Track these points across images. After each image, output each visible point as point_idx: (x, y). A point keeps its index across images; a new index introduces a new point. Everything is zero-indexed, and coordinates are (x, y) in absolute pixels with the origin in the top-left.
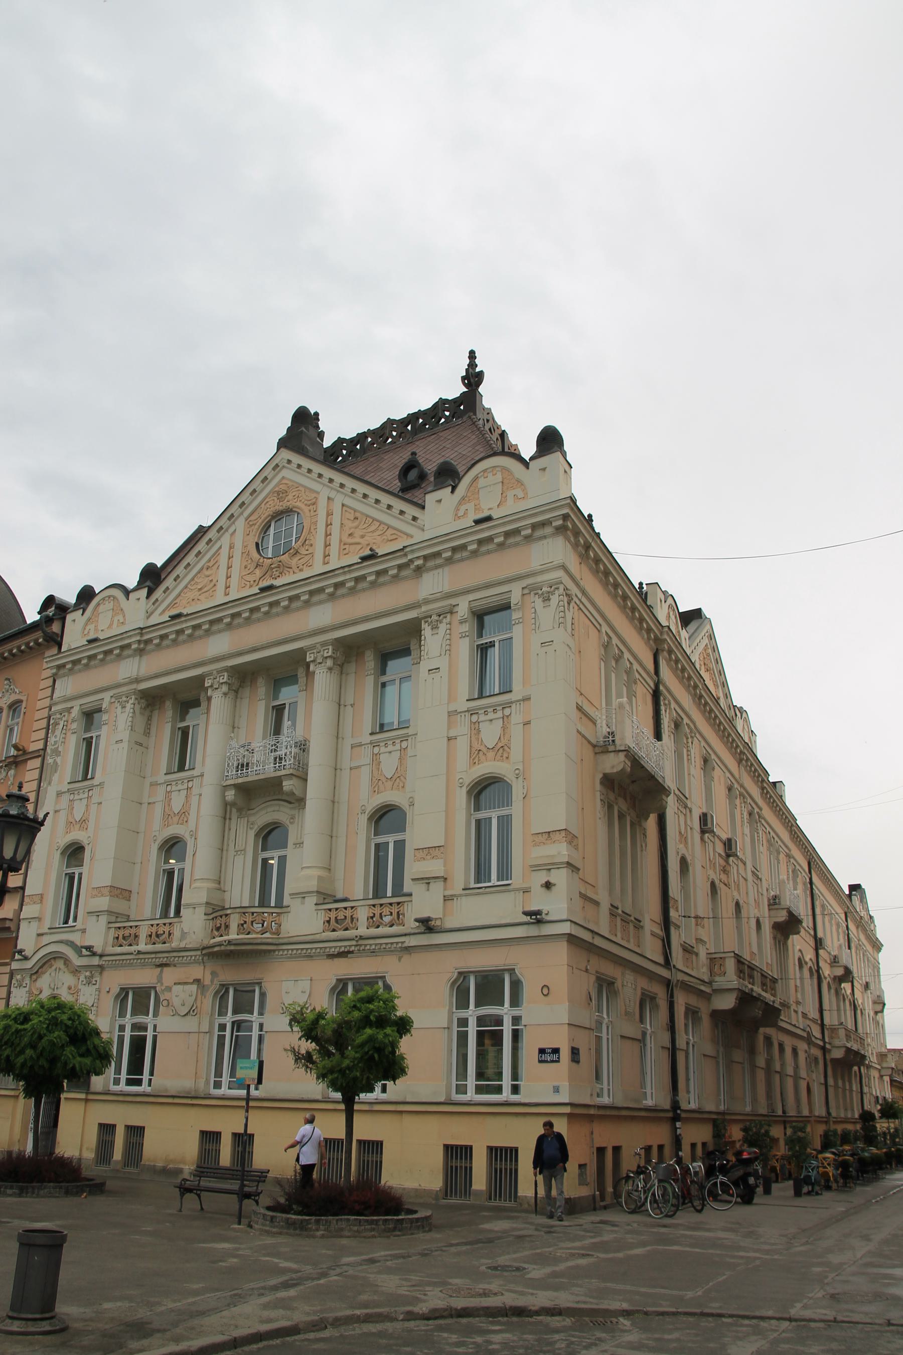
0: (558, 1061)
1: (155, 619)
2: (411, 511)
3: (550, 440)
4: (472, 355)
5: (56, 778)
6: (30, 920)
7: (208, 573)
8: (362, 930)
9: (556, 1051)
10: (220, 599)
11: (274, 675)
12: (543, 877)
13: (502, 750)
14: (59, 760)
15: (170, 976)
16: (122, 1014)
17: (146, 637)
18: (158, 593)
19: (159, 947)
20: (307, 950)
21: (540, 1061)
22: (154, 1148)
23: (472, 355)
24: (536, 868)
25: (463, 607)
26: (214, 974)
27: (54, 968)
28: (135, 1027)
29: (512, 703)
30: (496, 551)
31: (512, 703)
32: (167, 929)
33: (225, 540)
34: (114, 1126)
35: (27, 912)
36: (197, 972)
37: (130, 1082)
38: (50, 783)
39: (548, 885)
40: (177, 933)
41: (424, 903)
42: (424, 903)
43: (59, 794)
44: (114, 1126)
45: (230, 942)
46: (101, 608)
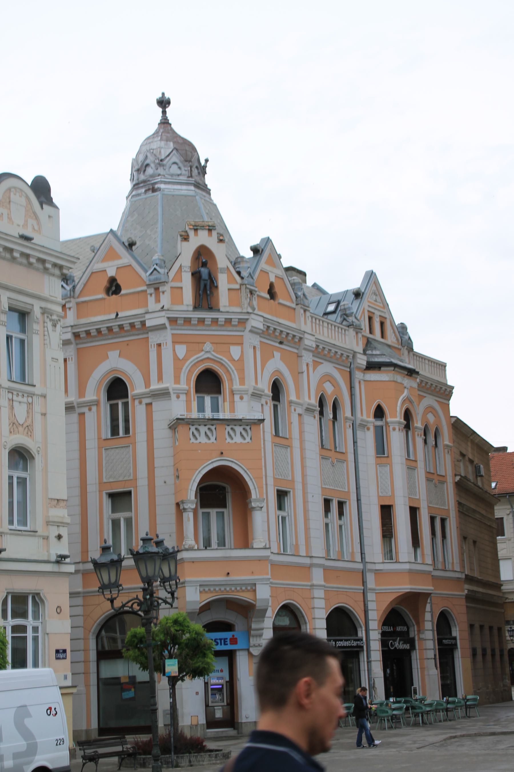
0: (65, 658)
3: (41, 188)
9: (65, 651)
12: (54, 531)
13: (29, 429)
21: (57, 658)
24: (48, 523)
29: (34, 395)
30: (25, 266)
31: (34, 395)
39: (59, 537)
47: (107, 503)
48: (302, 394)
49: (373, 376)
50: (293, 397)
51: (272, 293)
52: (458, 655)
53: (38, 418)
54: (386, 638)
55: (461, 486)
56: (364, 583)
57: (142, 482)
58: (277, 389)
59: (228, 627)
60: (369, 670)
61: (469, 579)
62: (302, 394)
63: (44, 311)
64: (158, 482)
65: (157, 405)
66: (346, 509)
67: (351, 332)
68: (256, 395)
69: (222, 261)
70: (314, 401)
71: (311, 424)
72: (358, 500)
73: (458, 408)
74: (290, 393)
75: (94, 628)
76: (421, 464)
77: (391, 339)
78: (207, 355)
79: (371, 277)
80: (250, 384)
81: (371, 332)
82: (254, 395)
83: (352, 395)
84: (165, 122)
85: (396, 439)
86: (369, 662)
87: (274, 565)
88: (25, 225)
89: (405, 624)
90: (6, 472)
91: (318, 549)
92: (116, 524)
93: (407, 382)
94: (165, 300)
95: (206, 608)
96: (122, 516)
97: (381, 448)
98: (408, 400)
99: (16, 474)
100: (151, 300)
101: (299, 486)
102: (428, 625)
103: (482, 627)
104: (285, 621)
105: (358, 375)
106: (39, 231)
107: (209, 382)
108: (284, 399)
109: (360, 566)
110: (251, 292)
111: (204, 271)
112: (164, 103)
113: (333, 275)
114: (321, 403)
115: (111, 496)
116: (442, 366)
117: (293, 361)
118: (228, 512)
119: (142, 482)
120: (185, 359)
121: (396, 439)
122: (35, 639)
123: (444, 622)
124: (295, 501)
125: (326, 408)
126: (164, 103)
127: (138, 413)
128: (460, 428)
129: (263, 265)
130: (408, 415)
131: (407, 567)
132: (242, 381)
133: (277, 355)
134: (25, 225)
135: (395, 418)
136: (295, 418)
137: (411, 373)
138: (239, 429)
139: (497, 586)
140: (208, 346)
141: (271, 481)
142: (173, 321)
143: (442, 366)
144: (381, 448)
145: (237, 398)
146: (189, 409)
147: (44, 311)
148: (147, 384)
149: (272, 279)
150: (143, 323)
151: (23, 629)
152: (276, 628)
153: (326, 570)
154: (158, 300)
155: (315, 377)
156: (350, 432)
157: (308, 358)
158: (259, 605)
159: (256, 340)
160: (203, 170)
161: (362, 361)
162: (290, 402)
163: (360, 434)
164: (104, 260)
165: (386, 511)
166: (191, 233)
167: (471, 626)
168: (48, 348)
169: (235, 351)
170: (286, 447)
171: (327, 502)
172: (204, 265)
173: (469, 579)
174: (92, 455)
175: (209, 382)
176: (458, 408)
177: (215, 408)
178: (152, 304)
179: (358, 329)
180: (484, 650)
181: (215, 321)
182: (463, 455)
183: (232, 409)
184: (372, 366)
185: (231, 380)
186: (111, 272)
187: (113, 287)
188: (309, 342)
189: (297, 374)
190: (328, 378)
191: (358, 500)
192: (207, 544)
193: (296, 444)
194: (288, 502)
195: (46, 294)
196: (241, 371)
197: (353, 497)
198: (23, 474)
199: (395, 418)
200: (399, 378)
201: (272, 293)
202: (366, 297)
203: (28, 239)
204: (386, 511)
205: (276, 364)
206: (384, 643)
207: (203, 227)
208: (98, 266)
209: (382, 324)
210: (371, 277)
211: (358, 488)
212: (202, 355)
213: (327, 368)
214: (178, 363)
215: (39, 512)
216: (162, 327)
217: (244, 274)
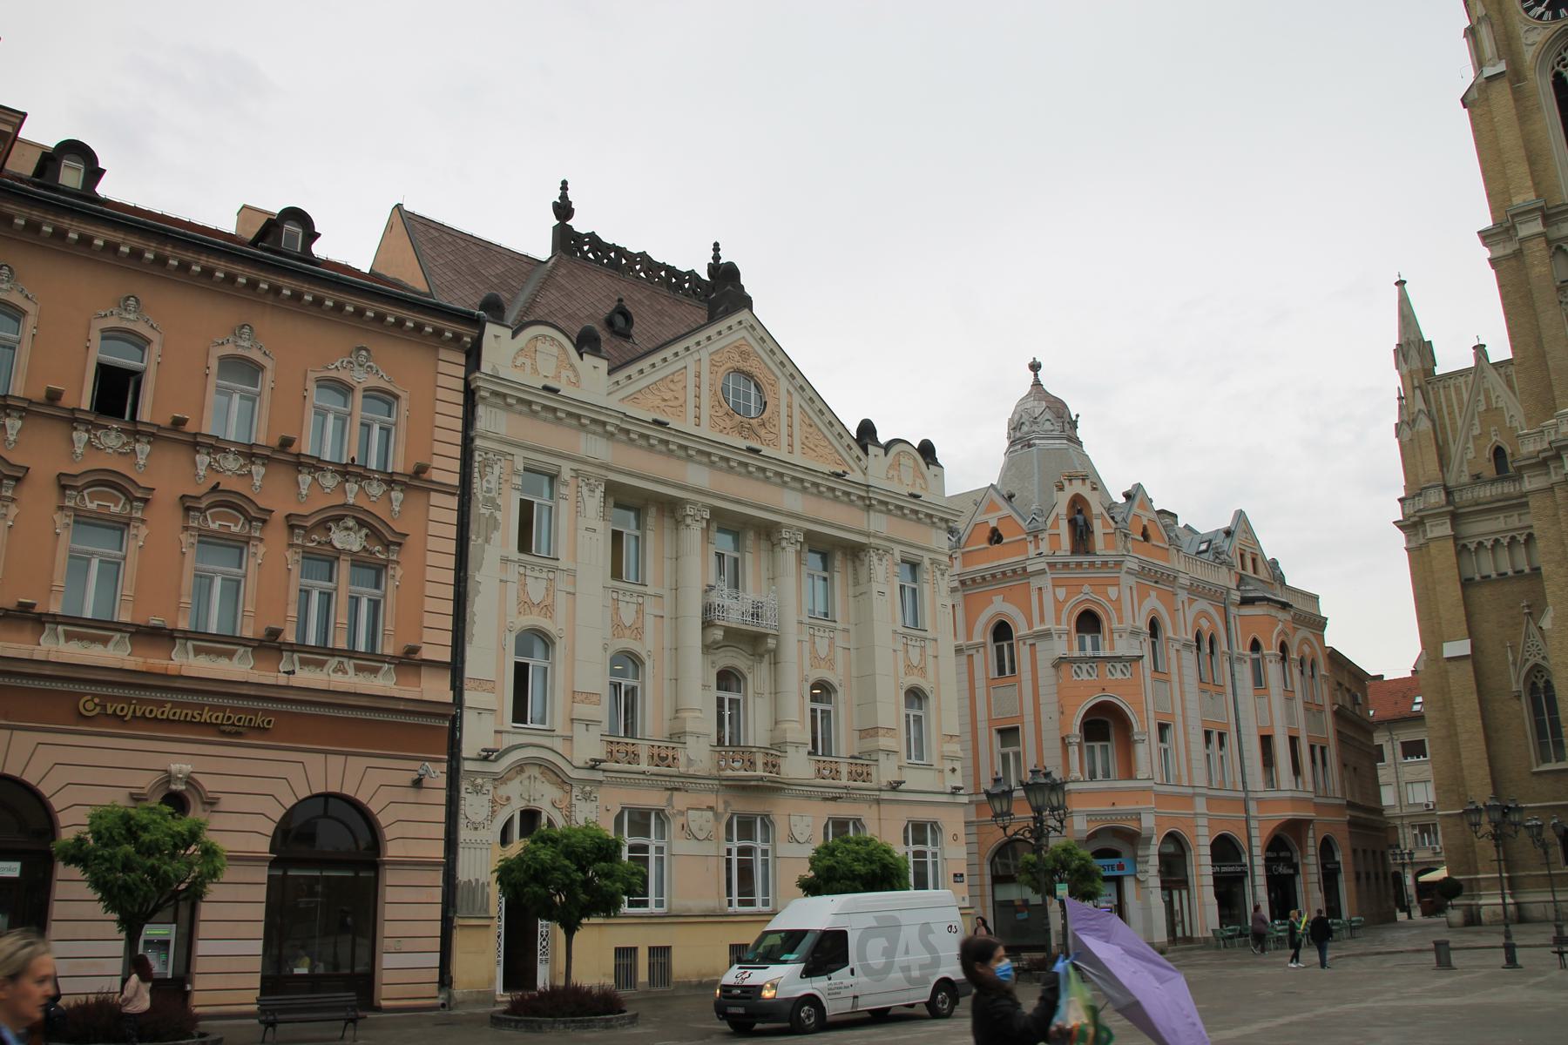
1: (613, 403)
2: (857, 450)
3: (927, 450)
4: (716, 247)
5: (496, 536)
6: (480, 711)
7: (672, 386)
8: (844, 782)
10: (690, 428)
11: (744, 530)
12: (948, 765)
13: (923, 671)
14: (498, 515)
15: (681, 801)
16: (729, 839)
17: (624, 426)
18: (620, 376)
19: (664, 770)
20: (805, 792)
22: (684, 965)
23: (716, 247)
24: (943, 757)
25: (897, 551)
26: (726, 803)
27: (525, 775)
28: (741, 851)
32: (670, 753)
33: (690, 361)
34: (635, 949)
35: (470, 698)
36: (711, 799)
37: (741, 903)
38: (487, 540)
39: (954, 770)
40: (682, 760)
41: (886, 772)
42: (886, 772)
43: (505, 560)
44: (635, 949)
45: (761, 779)
46: (539, 345)
47: (997, 739)
48: (1178, 630)
49: (1247, 611)
50: (1170, 634)
51: (1145, 535)
52: (1342, 878)
53: (930, 660)
54: (1269, 862)
55: (1339, 715)
56: (1247, 811)
57: (1029, 718)
58: (1154, 626)
59: (1115, 854)
60: (1254, 894)
61: (1351, 805)
62: (1178, 630)
63: (933, 562)
64: (1044, 718)
65: (1040, 645)
66: (1226, 740)
67: (1224, 568)
68: (1135, 633)
69: (1096, 508)
70: (1191, 637)
71: (1189, 658)
72: (1238, 731)
73: (1332, 638)
74: (1167, 630)
75: (989, 854)
76: (1298, 695)
77: (1263, 574)
78: (1086, 596)
79: (1240, 516)
80: (1128, 623)
81: (1243, 568)
82: (1132, 633)
83: (1228, 630)
84: (1037, 384)
85: (1273, 671)
86: (1254, 887)
87: (1157, 794)
88: (914, 485)
89: (1288, 849)
90: (903, 711)
91: (1200, 779)
92: (1005, 758)
93: (1281, 615)
94: (1044, 547)
95: (1093, 836)
96: (1010, 750)
97: (1259, 680)
98: (1283, 632)
99: (912, 712)
100: (1031, 547)
101: (1179, 719)
102: (1311, 851)
103: (1365, 851)
104: (1171, 849)
105: (1233, 610)
106: (926, 489)
107: (1089, 622)
108: (1162, 635)
109: (1243, 795)
110: (1126, 536)
111: (1080, 518)
112: (1035, 367)
113: (1203, 515)
114: (1198, 638)
115: (1000, 731)
116: (1316, 598)
117: (1169, 599)
118: (1112, 746)
119: (1029, 718)
120: (1065, 601)
121: (1273, 671)
122: (935, 864)
123: (1327, 847)
124: (1176, 734)
125: (1203, 643)
126: (1035, 367)
127: (1023, 653)
128: (1335, 658)
129: (1136, 510)
130: (1283, 647)
131: (1289, 794)
132: (1120, 620)
133: (1153, 594)
134: (914, 485)
135: (1271, 650)
136: (1173, 654)
137: (1285, 606)
138: (1119, 666)
139: (1379, 810)
140: (1086, 588)
141: (1152, 714)
142: (1052, 565)
143: (1316, 598)
144: (1259, 680)
145: (1116, 636)
146: (1071, 649)
147: (933, 562)
148: (1030, 626)
149: (1145, 522)
150: (1024, 569)
151: (923, 854)
152: (1160, 855)
153: (1209, 798)
154: (1037, 547)
155: (1191, 614)
156: (1227, 665)
157: (1183, 595)
158: (1144, 834)
159: (1132, 581)
160: (1074, 425)
161: (1236, 596)
162: (1168, 638)
163: (1237, 667)
164: (987, 511)
165: (1266, 741)
166: (1066, 483)
167: (1355, 851)
168: (938, 596)
169: (1113, 592)
170: (1166, 681)
171: (1208, 734)
172: (1080, 512)
173: (1351, 805)
174: (981, 692)
175: (1089, 622)
176: (1332, 638)
177: (1096, 647)
178: (1032, 551)
179: (1230, 566)
180: (1368, 874)
181: (1092, 564)
182: (1340, 684)
183: (1112, 648)
184: (1245, 601)
185: (1109, 619)
186: (993, 523)
187: (996, 537)
188: (1183, 580)
189: (1173, 612)
190: (1203, 614)
191: (1238, 731)
192: (1093, 776)
193: (1175, 678)
194: (1169, 734)
195: (934, 546)
196: (1119, 610)
197: (1233, 728)
198: (919, 713)
199: (1271, 650)
200: (1273, 612)
201: (1145, 535)
202: (1236, 536)
203: (916, 497)
204: (1266, 741)
205: (1153, 602)
206: (1268, 868)
207: (1077, 477)
208: (979, 519)
209: (1254, 560)
210: (1240, 516)
211: (1237, 720)
212: (1081, 597)
213: (1202, 604)
214: (1059, 605)
215: (934, 747)
216: (1043, 572)
217: (1118, 519)
